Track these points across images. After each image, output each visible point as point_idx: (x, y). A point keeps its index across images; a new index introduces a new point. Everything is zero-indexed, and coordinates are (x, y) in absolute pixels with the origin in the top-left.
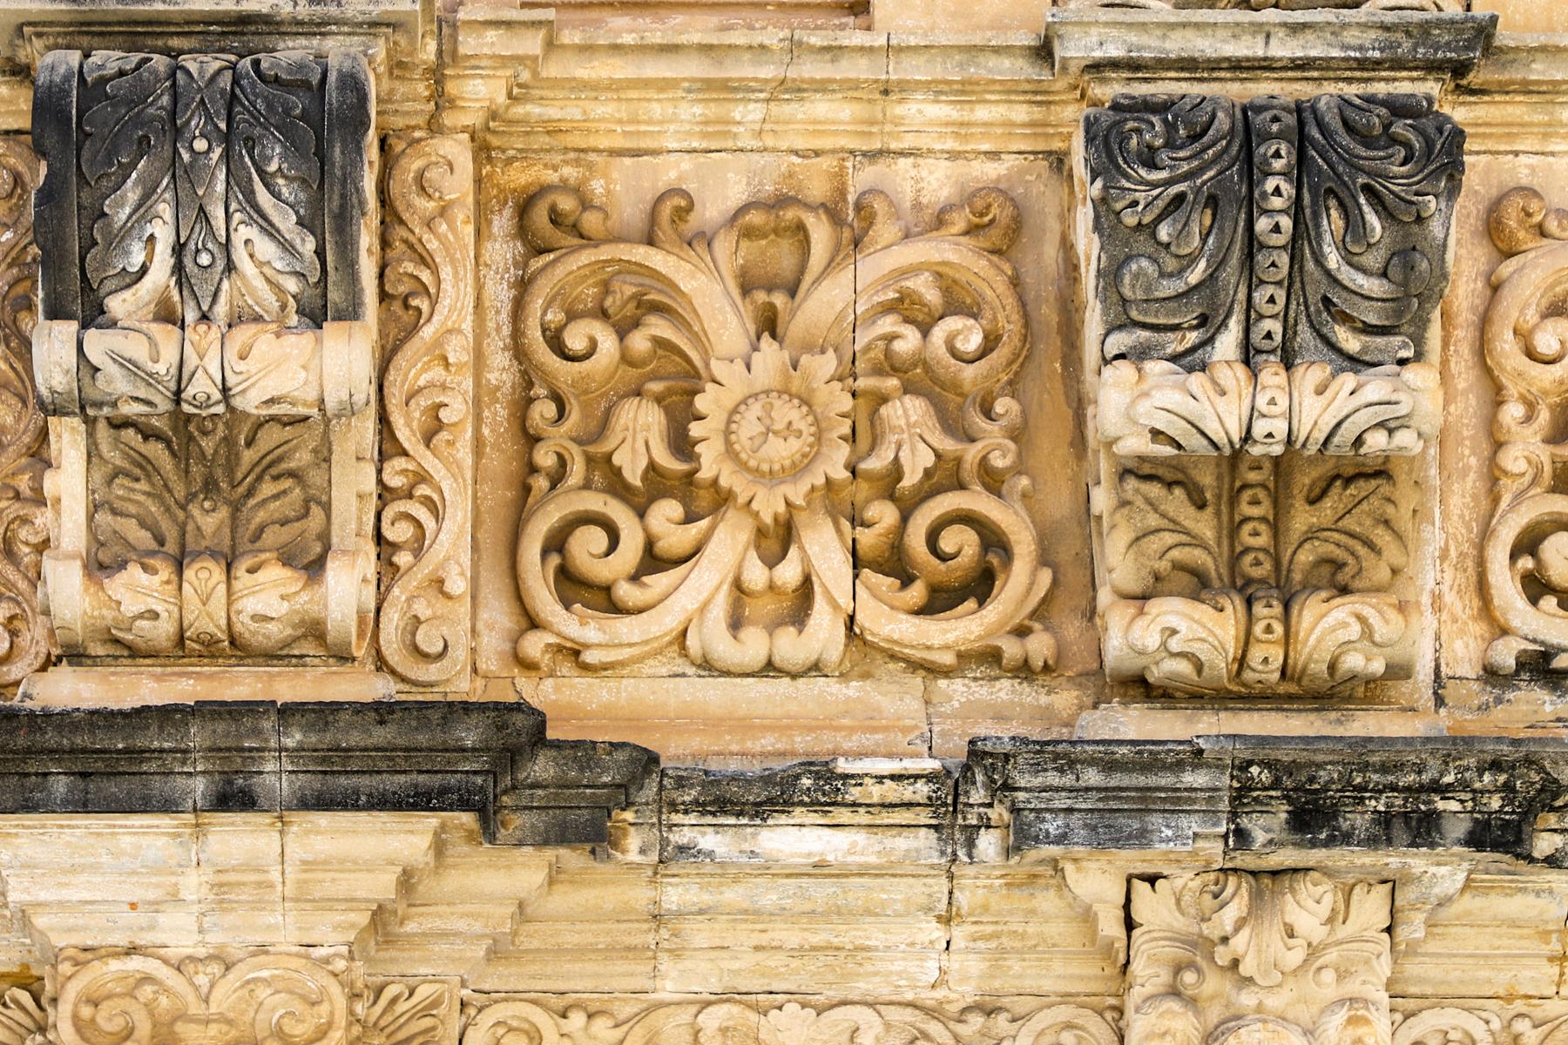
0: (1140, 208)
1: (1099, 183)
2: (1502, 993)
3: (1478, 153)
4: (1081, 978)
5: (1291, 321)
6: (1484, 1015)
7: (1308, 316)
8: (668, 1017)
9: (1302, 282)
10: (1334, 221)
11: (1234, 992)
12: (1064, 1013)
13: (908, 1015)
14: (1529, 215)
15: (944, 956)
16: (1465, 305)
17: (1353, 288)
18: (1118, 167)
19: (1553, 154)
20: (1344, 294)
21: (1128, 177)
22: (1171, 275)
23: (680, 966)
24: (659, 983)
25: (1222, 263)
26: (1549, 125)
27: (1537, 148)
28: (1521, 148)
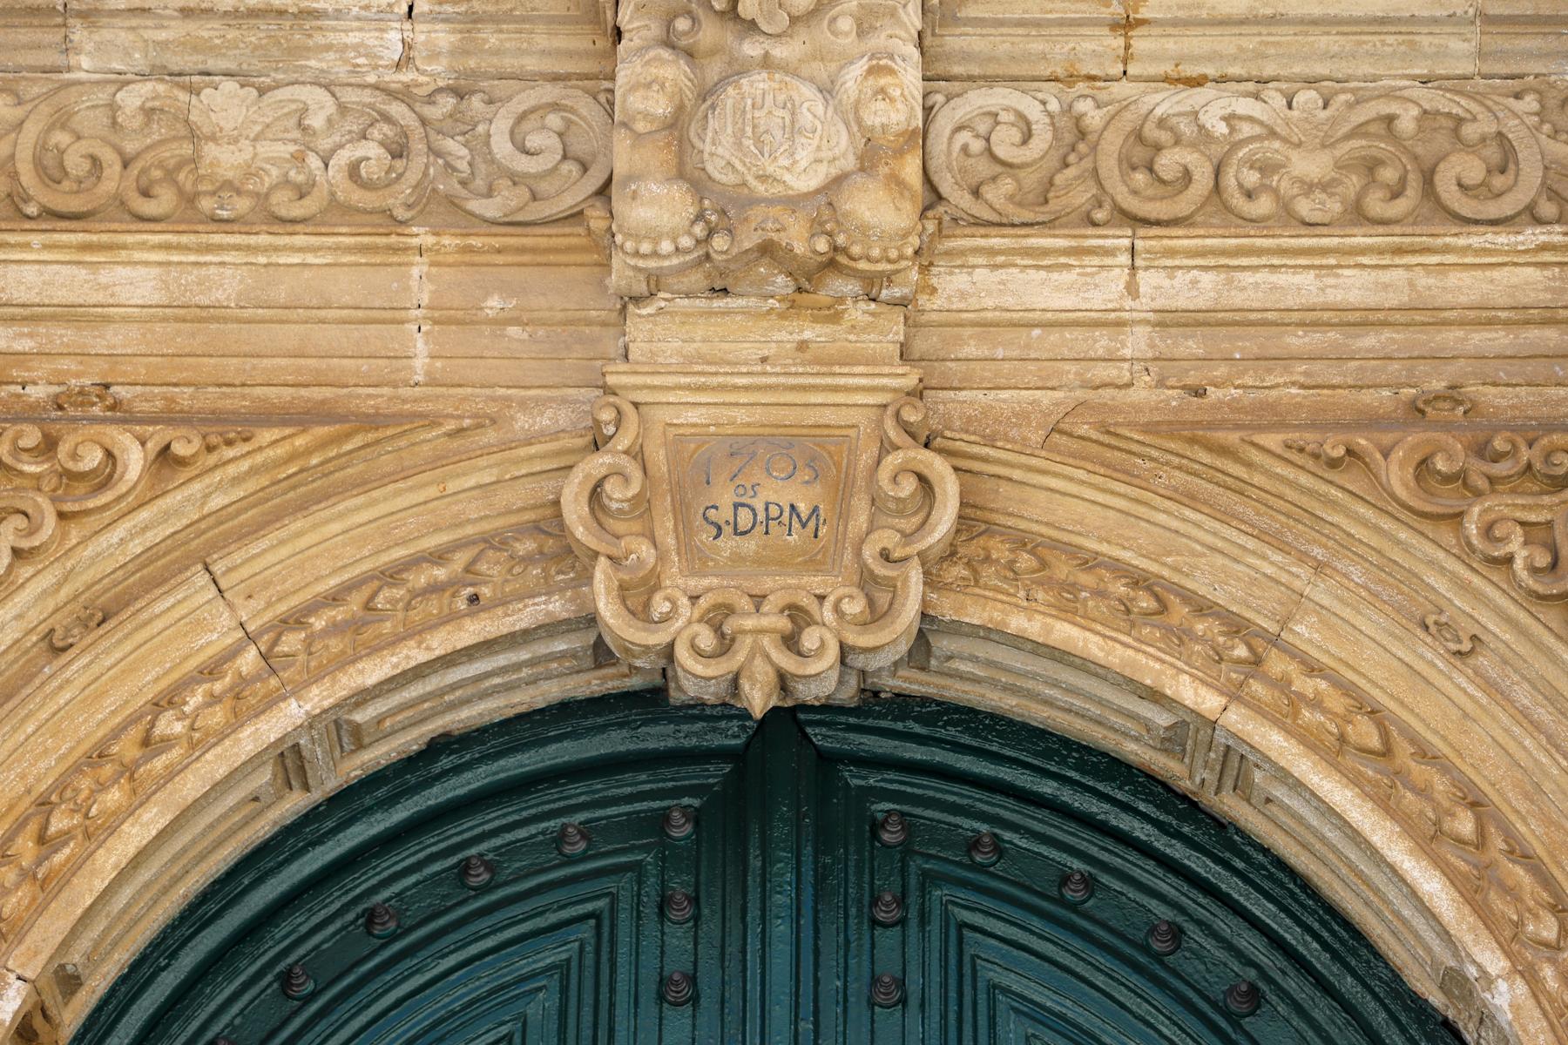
2: (1060, 72)
4: (571, 54)
6: (1040, 95)
8: (81, 95)
11: (735, 45)
12: (549, 92)
13: (367, 96)
15: (407, 26)
23: (96, 37)
24: (73, 60)
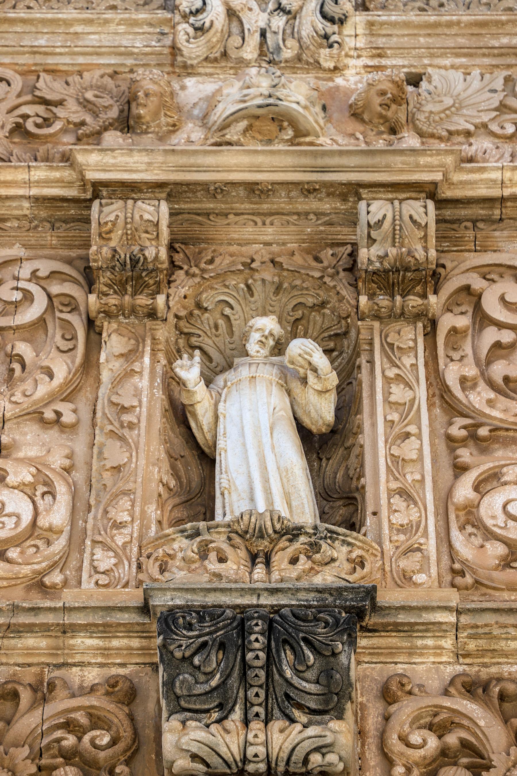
0: (183, 648)
1: (161, 637)
3: (376, 663)
5: (270, 709)
7: (278, 705)
9: (274, 687)
10: (287, 657)
14: (403, 685)
16: (372, 728)
17: (300, 687)
18: (172, 630)
19: (415, 663)
20: (296, 691)
21: (177, 635)
22: (202, 683)
25: (229, 676)
26: (411, 648)
27: (407, 660)
28: (399, 660)
